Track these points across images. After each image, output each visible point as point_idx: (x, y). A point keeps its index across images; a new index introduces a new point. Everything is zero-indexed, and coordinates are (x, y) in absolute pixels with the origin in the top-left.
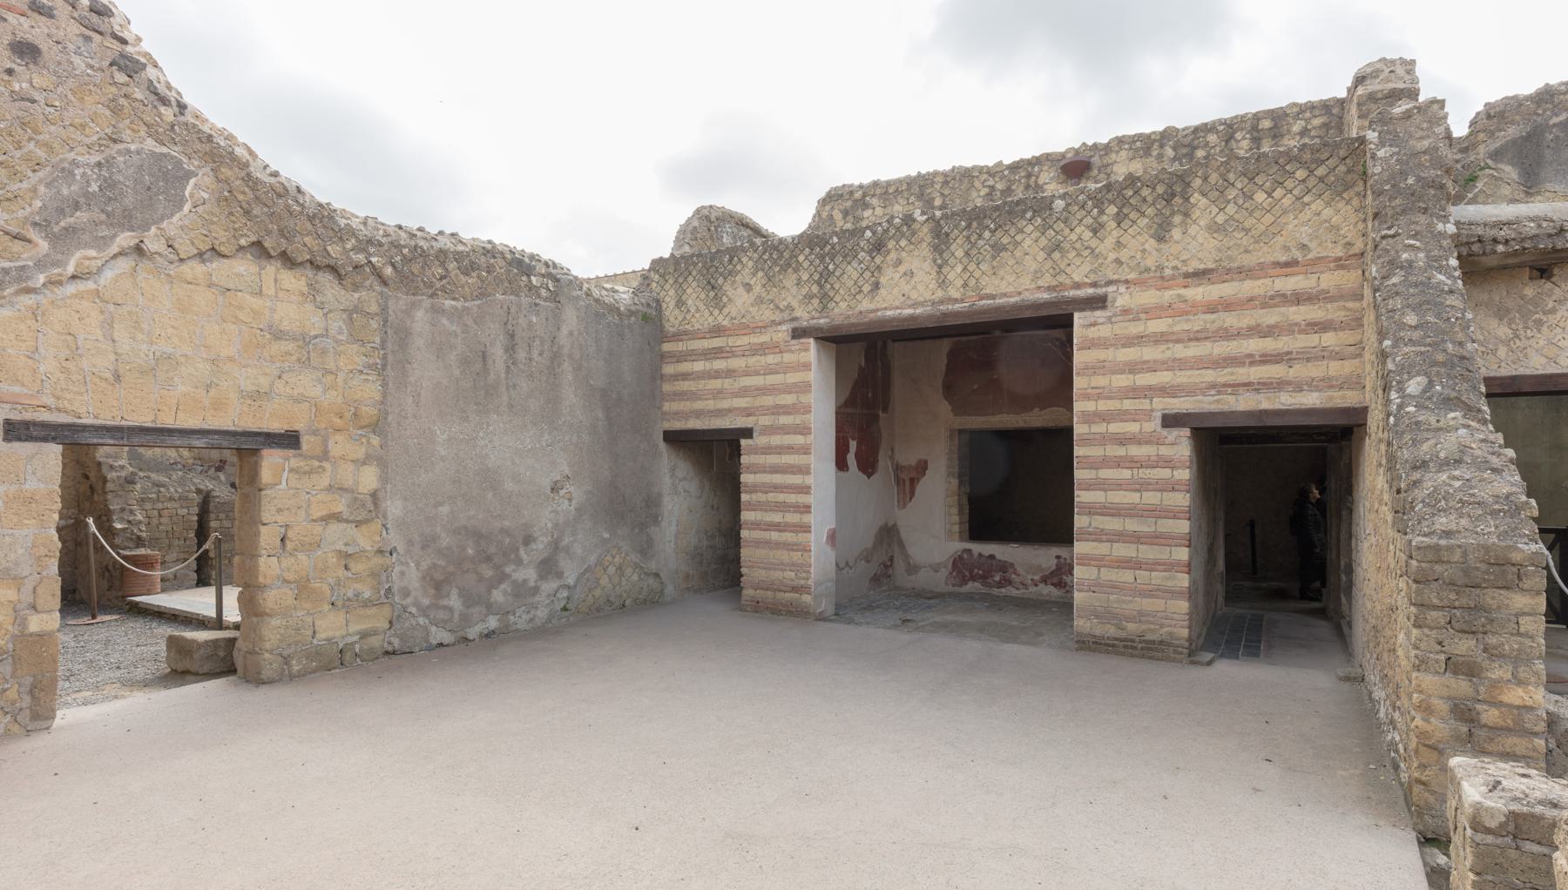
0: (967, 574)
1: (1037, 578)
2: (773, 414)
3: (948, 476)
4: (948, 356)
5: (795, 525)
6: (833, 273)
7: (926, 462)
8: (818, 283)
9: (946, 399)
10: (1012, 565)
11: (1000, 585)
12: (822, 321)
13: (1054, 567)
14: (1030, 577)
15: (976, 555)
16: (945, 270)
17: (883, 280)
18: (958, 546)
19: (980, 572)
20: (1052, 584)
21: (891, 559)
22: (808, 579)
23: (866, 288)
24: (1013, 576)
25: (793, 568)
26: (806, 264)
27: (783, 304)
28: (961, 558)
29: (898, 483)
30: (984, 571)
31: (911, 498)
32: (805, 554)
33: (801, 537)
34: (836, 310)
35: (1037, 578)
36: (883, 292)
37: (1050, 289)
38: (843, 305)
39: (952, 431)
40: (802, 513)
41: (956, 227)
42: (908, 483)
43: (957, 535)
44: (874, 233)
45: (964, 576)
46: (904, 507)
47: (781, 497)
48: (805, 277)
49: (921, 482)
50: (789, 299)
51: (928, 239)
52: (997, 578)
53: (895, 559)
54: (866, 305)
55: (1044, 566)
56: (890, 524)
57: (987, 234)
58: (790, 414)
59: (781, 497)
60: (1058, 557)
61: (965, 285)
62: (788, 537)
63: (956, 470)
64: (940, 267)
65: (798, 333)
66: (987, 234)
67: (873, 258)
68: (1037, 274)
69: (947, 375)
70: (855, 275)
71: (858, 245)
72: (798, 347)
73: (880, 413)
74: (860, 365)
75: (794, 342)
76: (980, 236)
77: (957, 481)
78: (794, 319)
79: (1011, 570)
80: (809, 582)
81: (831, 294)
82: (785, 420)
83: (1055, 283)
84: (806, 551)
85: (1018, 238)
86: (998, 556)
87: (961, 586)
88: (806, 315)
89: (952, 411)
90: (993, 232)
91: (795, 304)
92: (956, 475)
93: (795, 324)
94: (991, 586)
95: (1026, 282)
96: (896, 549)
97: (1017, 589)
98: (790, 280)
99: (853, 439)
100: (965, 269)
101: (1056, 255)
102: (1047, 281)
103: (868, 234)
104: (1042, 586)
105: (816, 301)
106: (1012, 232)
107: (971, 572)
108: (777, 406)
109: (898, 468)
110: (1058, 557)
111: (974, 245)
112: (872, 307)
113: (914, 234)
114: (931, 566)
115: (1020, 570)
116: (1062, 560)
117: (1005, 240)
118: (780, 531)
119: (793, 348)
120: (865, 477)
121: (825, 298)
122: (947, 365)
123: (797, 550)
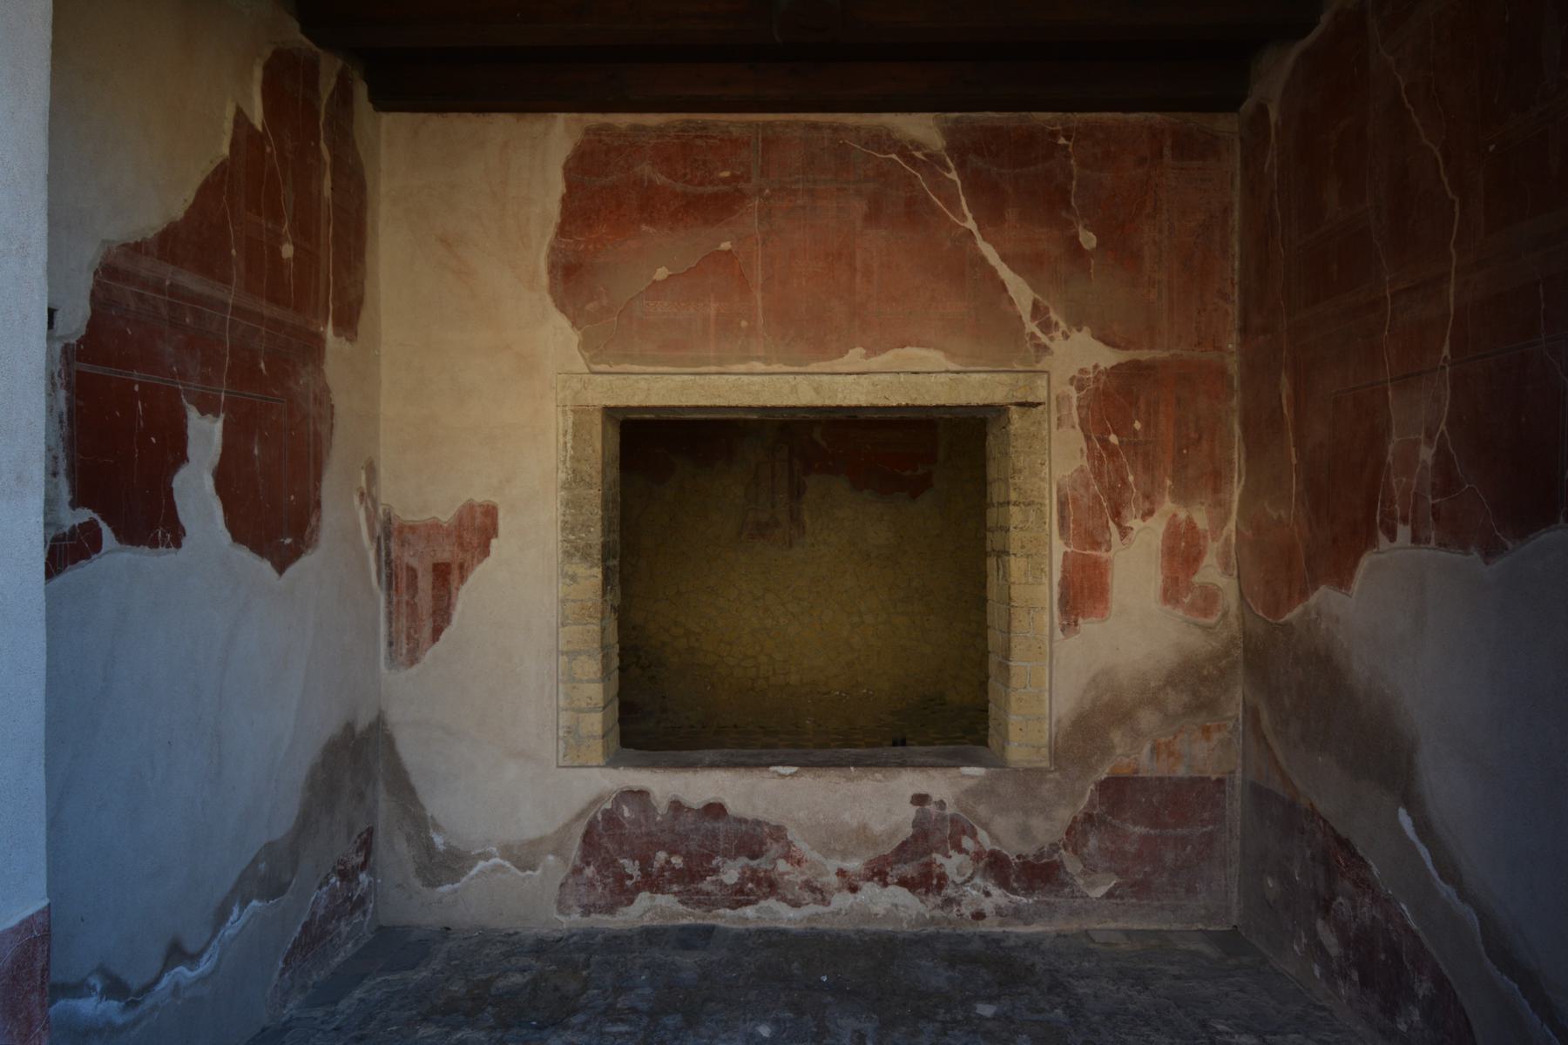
0: (632, 867)
1: (854, 865)
3: (568, 555)
4: (567, 170)
7: (491, 512)
9: (563, 309)
10: (778, 833)
11: (739, 896)
13: (908, 831)
14: (833, 864)
15: (662, 807)
19: (677, 861)
20: (903, 882)
21: (366, 843)
24: (782, 866)
28: (611, 818)
29: (391, 583)
30: (687, 857)
31: (437, 633)
35: (854, 865)
39: (580, 411)
42: (425, 583)
43: (598, 745)
45: (622, 876)
46: (413, 660)
49: (471, 579)
52: (731, 874)
53: (380, 839)
55: (878, 828)
56: (362, 724)
60: (920, 799)
63: (595, 536)
69: (562, 231)
73: (329, 331)
74: (241, 119)
77: (597, 572)
79: (774, 848)
86: (735, 807)
87: (610, 909)
89: (584, 345)
92: (596, 554)
94: (708, 902)
96: (384, 805)
97: (796, 904)
99: (207, 407)
104: (870, 890)
107: (646, 862)
109: (389, 532)
110: (920, 799)
114: (507, 851)
115: (802, 847)
116: (932, 808)
120: (266, 566)
122: (565, 200)
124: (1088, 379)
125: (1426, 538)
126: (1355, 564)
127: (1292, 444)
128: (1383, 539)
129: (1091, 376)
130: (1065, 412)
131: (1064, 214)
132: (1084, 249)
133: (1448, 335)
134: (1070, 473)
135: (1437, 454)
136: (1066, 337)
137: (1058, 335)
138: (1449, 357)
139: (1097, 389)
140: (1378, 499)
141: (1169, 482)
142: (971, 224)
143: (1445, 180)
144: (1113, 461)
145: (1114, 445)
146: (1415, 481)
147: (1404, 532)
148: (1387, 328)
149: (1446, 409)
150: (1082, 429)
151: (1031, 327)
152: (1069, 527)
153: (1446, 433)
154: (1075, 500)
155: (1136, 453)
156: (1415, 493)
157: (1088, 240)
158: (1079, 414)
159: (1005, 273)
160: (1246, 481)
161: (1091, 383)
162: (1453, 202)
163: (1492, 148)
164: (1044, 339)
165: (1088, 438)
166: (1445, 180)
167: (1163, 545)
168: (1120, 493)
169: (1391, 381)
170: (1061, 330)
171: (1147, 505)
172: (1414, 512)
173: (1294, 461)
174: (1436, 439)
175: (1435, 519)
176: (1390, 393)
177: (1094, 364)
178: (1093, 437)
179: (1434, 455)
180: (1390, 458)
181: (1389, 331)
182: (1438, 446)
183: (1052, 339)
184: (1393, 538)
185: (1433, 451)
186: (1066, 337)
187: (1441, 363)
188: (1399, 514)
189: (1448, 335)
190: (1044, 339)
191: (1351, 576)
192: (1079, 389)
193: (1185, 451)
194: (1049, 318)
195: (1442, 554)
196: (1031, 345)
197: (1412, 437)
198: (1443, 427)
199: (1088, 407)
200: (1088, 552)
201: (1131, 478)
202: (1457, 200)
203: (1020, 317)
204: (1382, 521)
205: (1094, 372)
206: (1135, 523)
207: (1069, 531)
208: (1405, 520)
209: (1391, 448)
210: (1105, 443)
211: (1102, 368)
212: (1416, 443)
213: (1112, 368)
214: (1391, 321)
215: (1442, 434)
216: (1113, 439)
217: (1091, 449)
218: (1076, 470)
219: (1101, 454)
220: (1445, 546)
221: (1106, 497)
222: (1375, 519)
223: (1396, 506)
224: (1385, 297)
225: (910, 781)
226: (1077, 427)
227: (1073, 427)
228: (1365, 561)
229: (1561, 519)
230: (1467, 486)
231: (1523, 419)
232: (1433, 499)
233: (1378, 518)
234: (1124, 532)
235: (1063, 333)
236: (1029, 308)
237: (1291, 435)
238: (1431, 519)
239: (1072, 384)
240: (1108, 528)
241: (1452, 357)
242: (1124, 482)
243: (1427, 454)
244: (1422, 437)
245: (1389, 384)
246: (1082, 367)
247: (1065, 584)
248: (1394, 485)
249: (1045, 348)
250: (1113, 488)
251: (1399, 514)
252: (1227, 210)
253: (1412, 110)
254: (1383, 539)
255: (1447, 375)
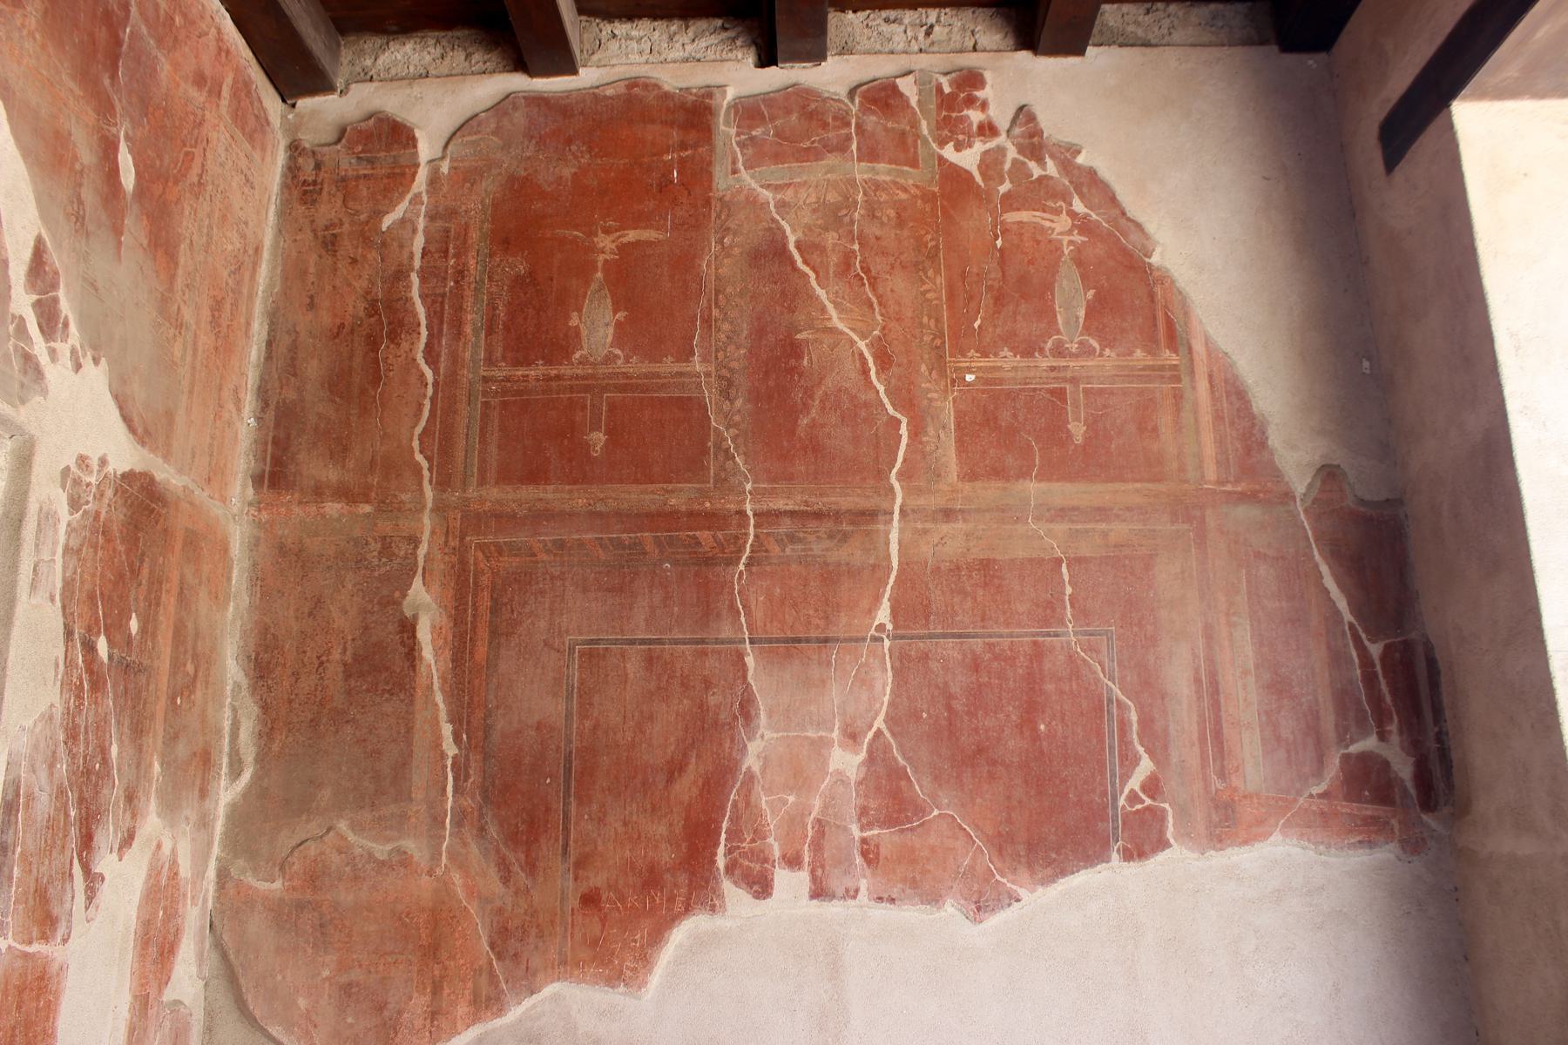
124: (88, 485)
125: (847, 891)
126: (657, 937)
127: (443, 714)
128: (734, 895)
129: (93, 480)
130: (46, 556)
131: (107, 82)
132: (121, 183)
133: (887, 595)
134: (29, 723)
135: (871, 759)
136: (78, 367)
137: (64, 349)
138: (890, 627)
139: (97, 515)
140: (721, 828)
141: (157, 767)
143: (881, 389)
144: (96, 703)
145: (102, 663)
146: (817, 803)
147: (790, 884)
148: (743, 560)
149: (886, 699)
150: (64, 608)
151: (23, 302)
152: (10, 878)
153: (888, 735)
154: (30, 797)
155: (126, 689)
156: (819, 821)
158: (65, 568)
160: (257, 778)
161: (91, 499)
162: (899, 422)
163: (970, 378)
164: (39, 346)
165: (69, 633)
166: (881, 389)
167: (138, 918)
168: (96, 785)
169: (751, 643)
170: (70, 341)
171: (128, 822)
172: (817, 847)
173: (450, 749)
174: (867, 740)
175: (869, 862)
176: (750, 661)
177: (100, 454)
178: (77, 636)
179: (863, 763)
180: (751, 761)
181: (747, 565)
182: (870, 752)
183: (53, 353)
184: (761, 886)
185: (863, 755)
186: (78, 367)
187: (873, 632)
188: (777, 853)
189: (887, 595)
190: (39, 346)
191: (645, 960)
192: (74, 504)
193: (179, 701)
194: (55, 300)
195: (882, 912)
196: (16, 347)
197: (811, 734)
198: (879, 723)
199: (79, 551)
200: (35, 948)
201: (114, 750)
202: (904, 421)
203: (5, 263)
204: (730, 869)
205: (99, 471)
206: (106, 863)
207: (10, 886)
208: (793, 862)
209: (754, 748)
210: (90, 648)
211: (110, 469)
212: (821, 746)
213: (124, 476)
214: (752, 551)
215: (879, 733)
216: (102, 645)
217: (69, 663)
218: (42, 716)
219: (81, 683)
220: (892, 900)
221: (76, 796)
222: (714, 862)
223: (771, 840)
224: (742, 513)
226: (58, 598)
227: (52, 599)
228: (680, 934)
229: (1115, 856)
230: (936, 812)
231: (1042, 727)
232: (862, 829)
233: (721, 862)
235: (73, 351)
236: (27, 254)
237: (439, 698)
238: (859, 860)
239: (63, 487)
240: (71, 875)
241: (894, 628)
242: (105, 761)
243: (847, 762)
244: (836, 734)
245: (748, 645)
246: (85, 453)
248: (764, 806)
249: (39, 374)
250: (88, 772)
251: (777, 853)
252: (258, 250)
253: (812, 275)
254: (734, 895)
255: (886, 651)
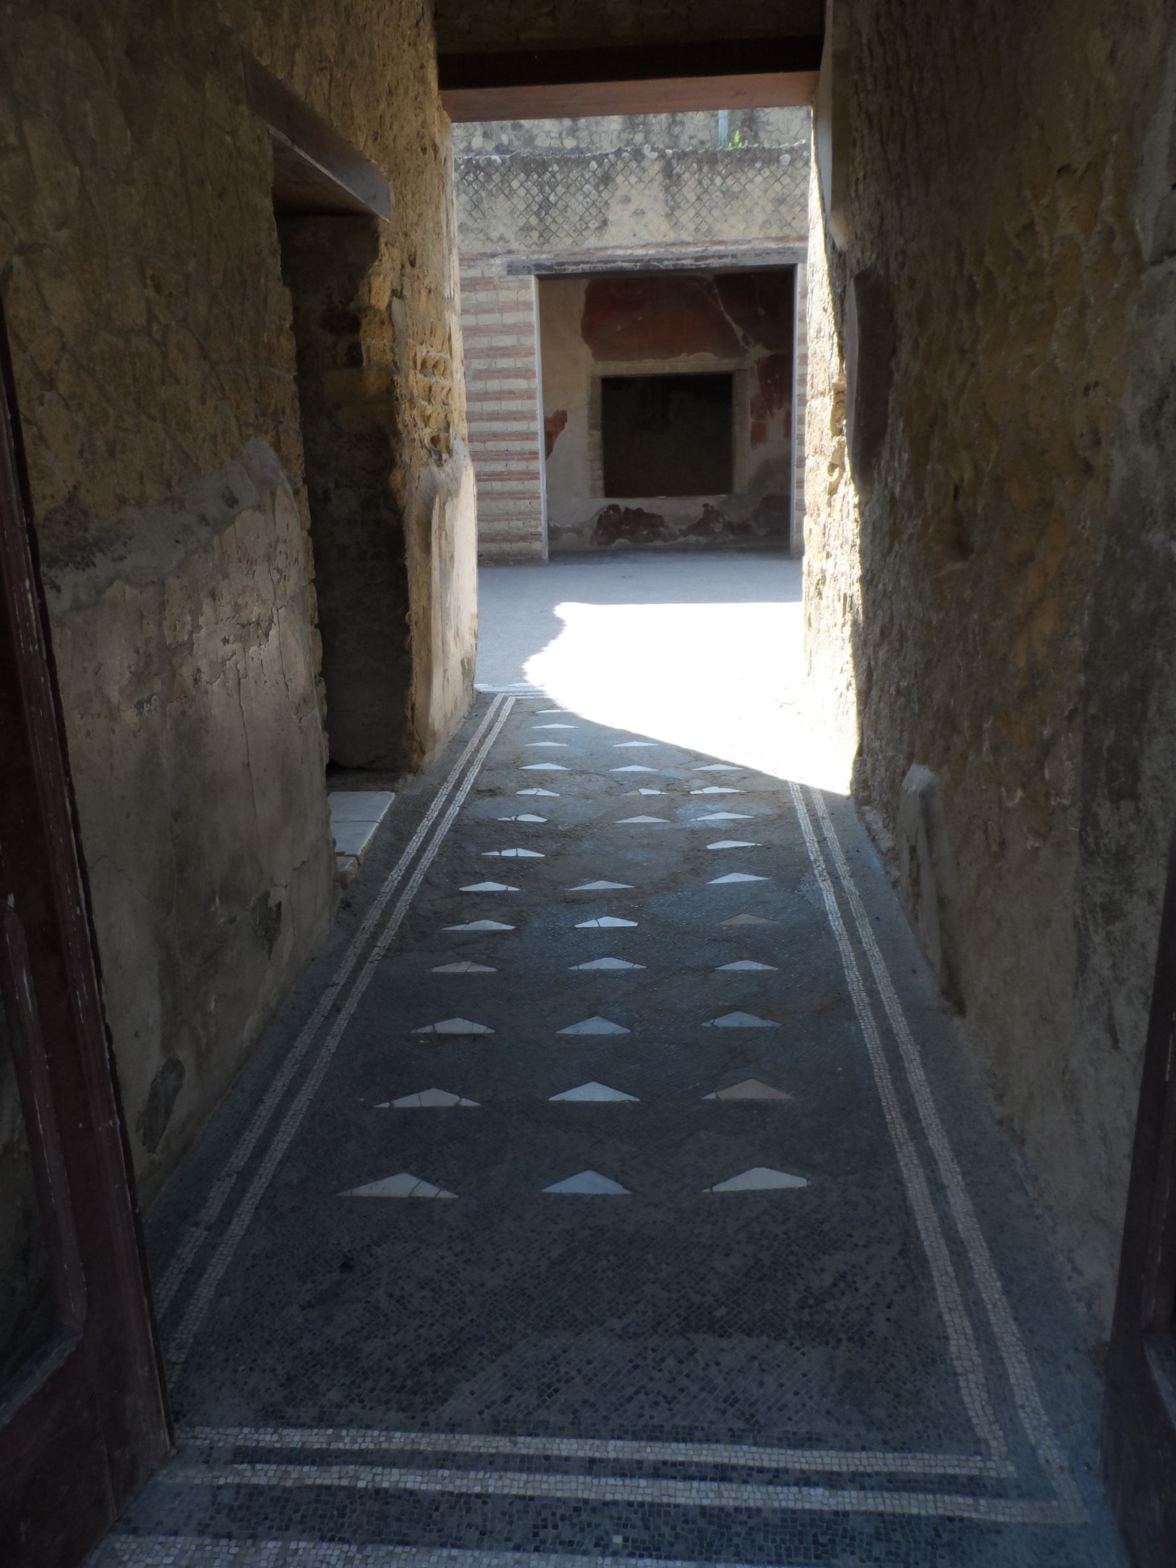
2: (489, 356)
5: (521, 473)
6: (555, 205)
8: (537, 214)
12: (544, 256)
16: (677, 213)
17: (612, 217)
18: (604, 502)
22: (537, 527)
23: (593, 225)
25: (520, 517)
26: (522, 192)
27: (495, 235)
32: (534, 502)
33: (529, 485)
34: (559, 246)
36: (611, 229)
37: (778, 239)
38: (568, 241)
40: (527, 459)
41: (688, 169)
44: (600, 164)
47: (502, 446)
48: (522, 206)
50: (502, 229)
51: (660, 178)
54: (592, 242)
57: (718, 180)
58: (508, 356)
59: (502, 446)
61: (697, 230)
62: (514, 486)
63: (599, 420)
64: (672, 209)
65: (512, 269)
66: (718, 180)
67: (600, 193)
68: (766, 224)
70: (580, 209)
71: (582, 175)
72: (515, 284)
75: (511, 278)
76: (712, 180)
78: (510, 252)
80: (539, 530)
81: (554, 227)
82: (503, 363)
83: (781, 235)
84: (535, 498)
85: (749, 187)
88: (525, 251)
90: (724, 178)
91: (509, 235)
93: (513, 257)
95: (755, 232)
98: (501, 206)
100: (697, 214)
101: (783, 209)
102: (774, 232)
103: (594, 165)
105: (535, 234)
106: (743, 181)
108: (492, 348)
110: (705, 506)
111: (706, 191)
112: (601, 244)
113: (644, 170)
117: (736, 188)
118: (502, 480)
119: (510, 284)
121: (545, 234)
122: (587, 304)
123: (524, 498)
142: (722, 308)
151: (742, 344)
157: (761, 312)
159: (734, 325)
225: (702, 500)
234: (772, 414)
247: (753, 433)
